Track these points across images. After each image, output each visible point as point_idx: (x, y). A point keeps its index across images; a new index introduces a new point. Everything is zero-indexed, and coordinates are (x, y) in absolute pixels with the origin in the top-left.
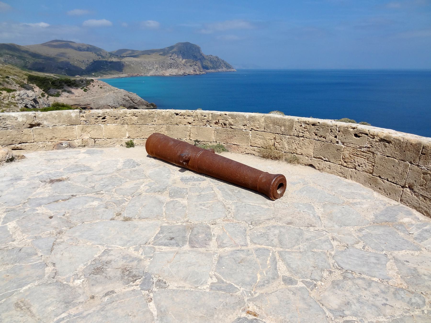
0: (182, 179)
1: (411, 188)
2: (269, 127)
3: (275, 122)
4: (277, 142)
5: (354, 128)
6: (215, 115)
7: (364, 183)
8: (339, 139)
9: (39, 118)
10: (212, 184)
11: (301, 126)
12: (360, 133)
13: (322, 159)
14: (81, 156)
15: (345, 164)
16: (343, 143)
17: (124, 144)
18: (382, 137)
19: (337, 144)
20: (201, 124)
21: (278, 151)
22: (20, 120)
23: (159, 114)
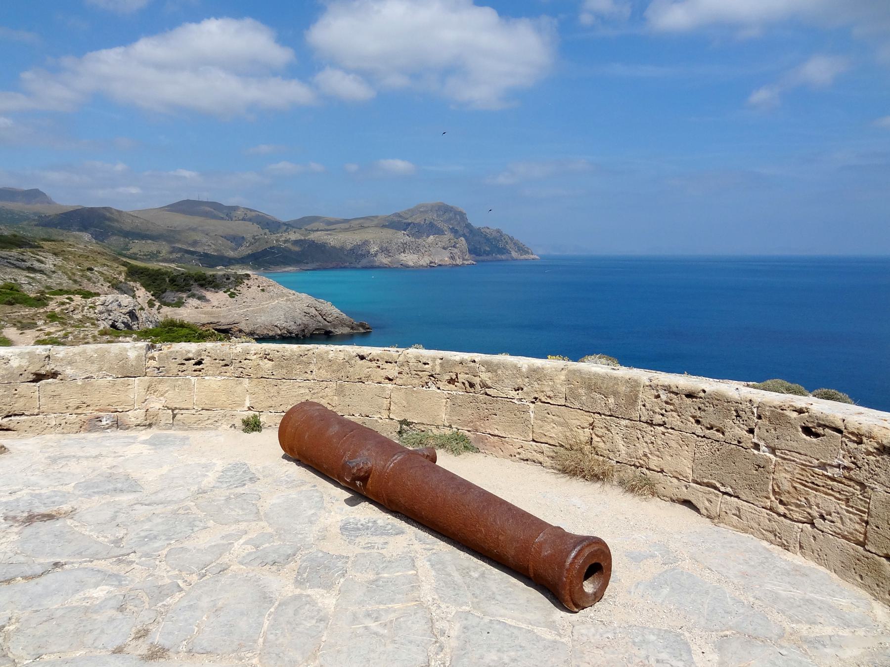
0: (344, 528)
2: (576, 397)
3: (593, 385)
5: (800, 411)
6: (448, 361)
7: (845, 569)
8: (760, 438)
9: (56, 360)
10: (417, 546)
11: (658, 397)
12: (819, 425)
13: (716, 488)
14: (131, 451)
15: (782, 509)
16: (773, 451)
17: (239, 424)
19: (756, 452)
20: (416, 381)
21: (601, 458)
22: (15, 363)
23: (320, 357)
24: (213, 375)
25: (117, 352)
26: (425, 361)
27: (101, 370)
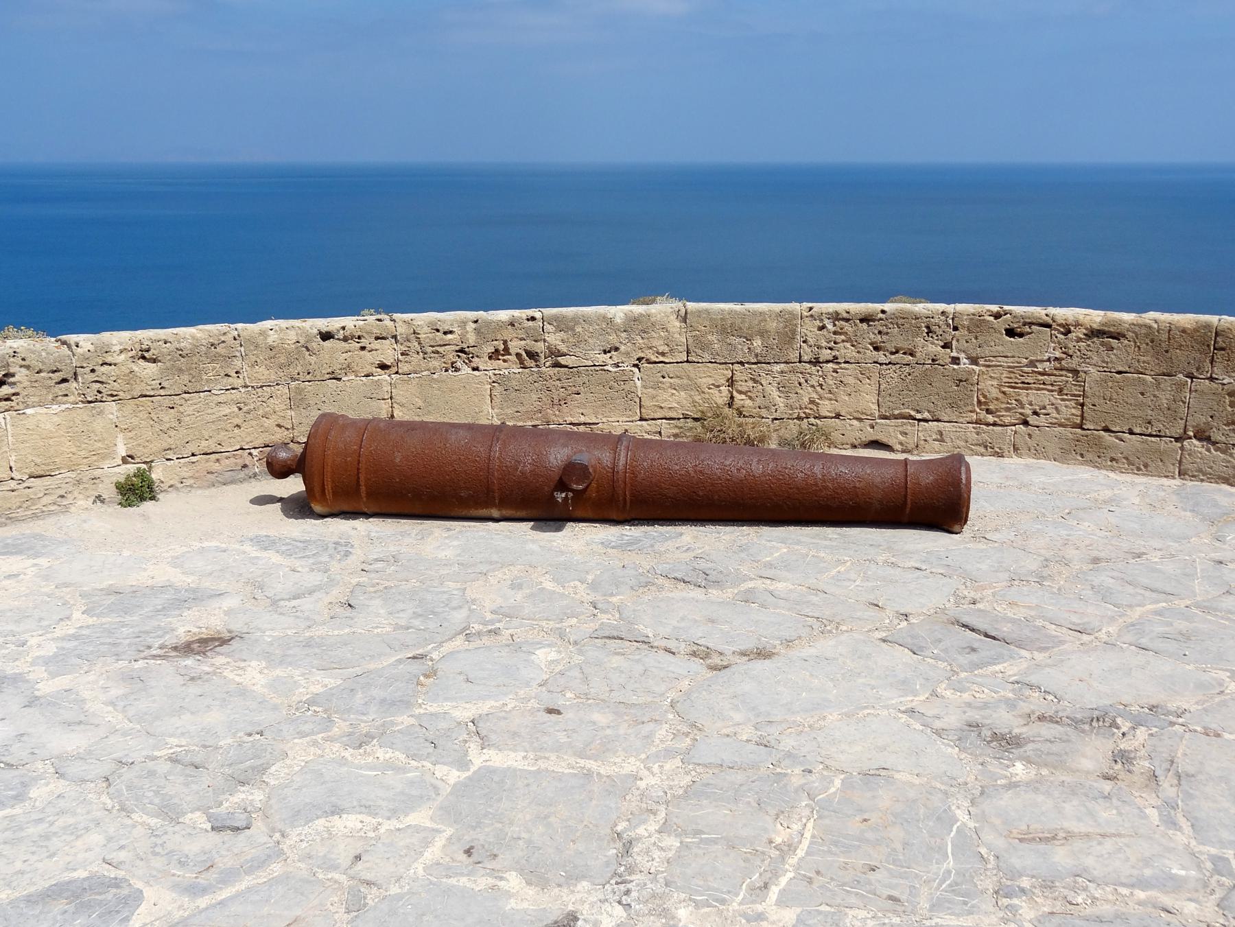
1: (1202, 436)
2: (705, 347)
3: (726, 328)
4: (740, 392)
7: (1063, 456)
8: (959, 350)
15: (990, 419)
16: (974, 361)
17: (109, 491)
18: (1095, 326)
20: (436, 363)
21: (751, 420)
23: (253, 343)
26: (447, 328)
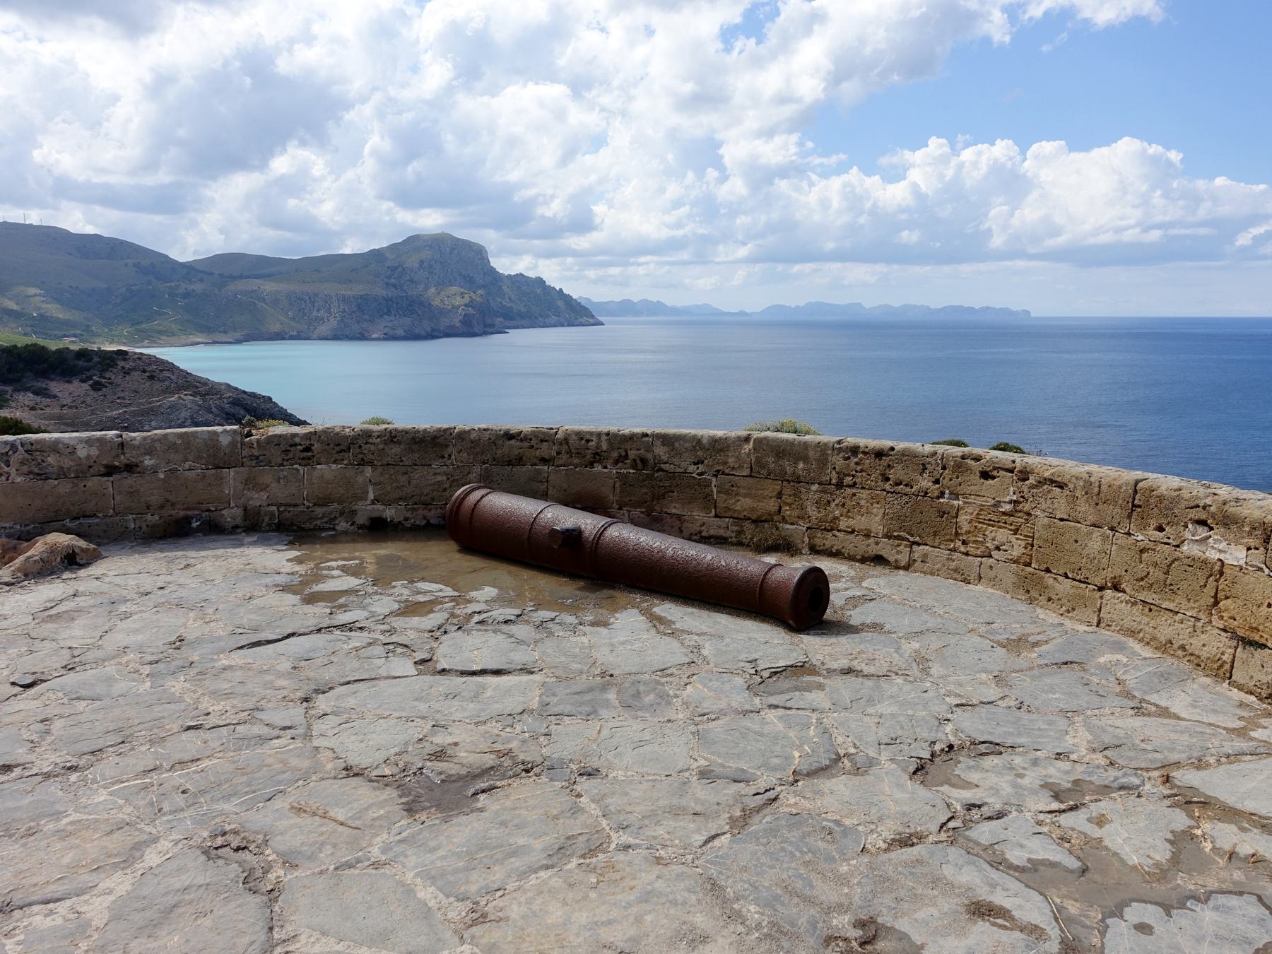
2: (763, 466)
4: (787, 504)
12: (995, 468)
20: (576, 461)
24: (327, 463)
25: (206, 437)
27: (186, 460)
